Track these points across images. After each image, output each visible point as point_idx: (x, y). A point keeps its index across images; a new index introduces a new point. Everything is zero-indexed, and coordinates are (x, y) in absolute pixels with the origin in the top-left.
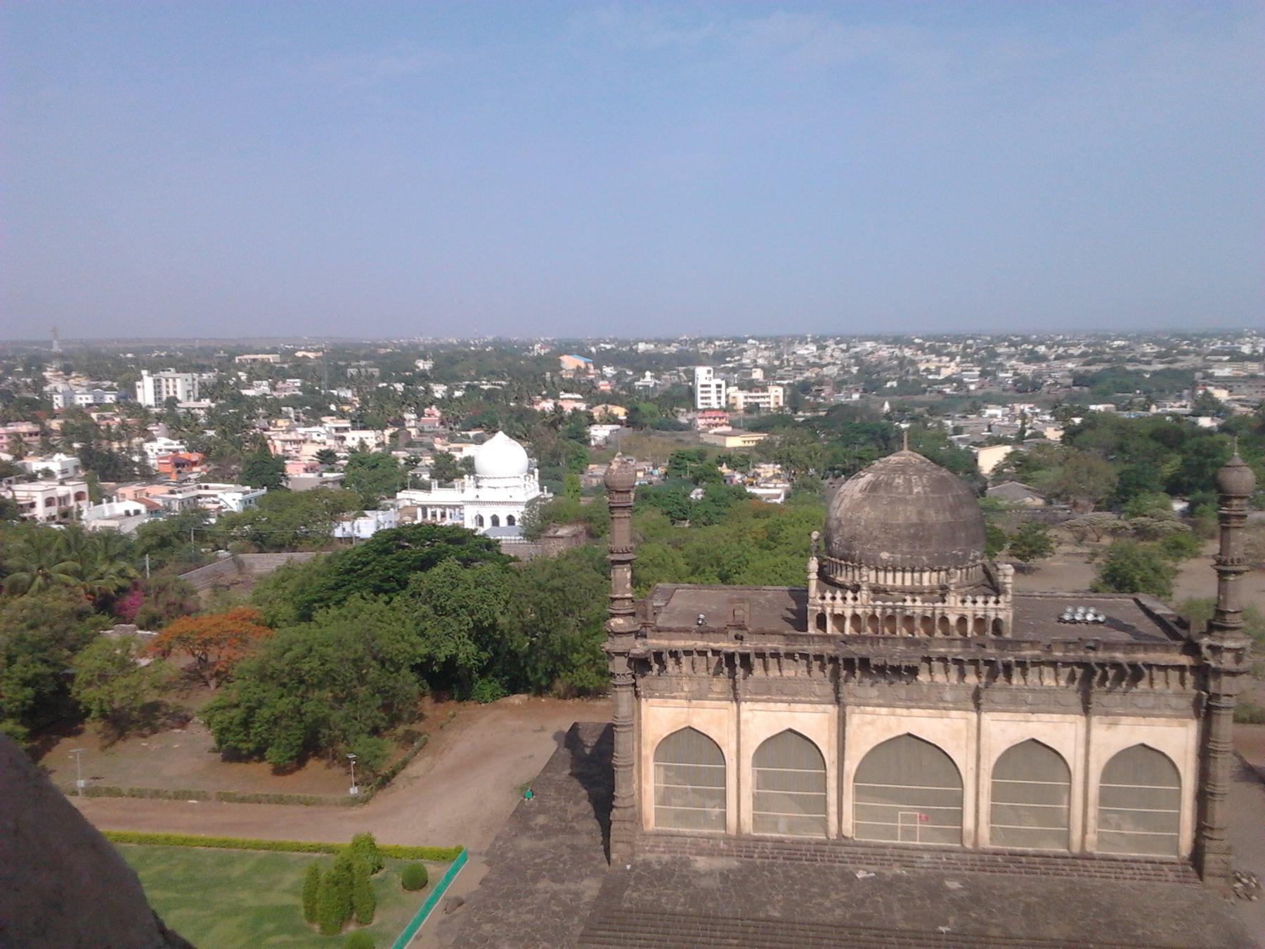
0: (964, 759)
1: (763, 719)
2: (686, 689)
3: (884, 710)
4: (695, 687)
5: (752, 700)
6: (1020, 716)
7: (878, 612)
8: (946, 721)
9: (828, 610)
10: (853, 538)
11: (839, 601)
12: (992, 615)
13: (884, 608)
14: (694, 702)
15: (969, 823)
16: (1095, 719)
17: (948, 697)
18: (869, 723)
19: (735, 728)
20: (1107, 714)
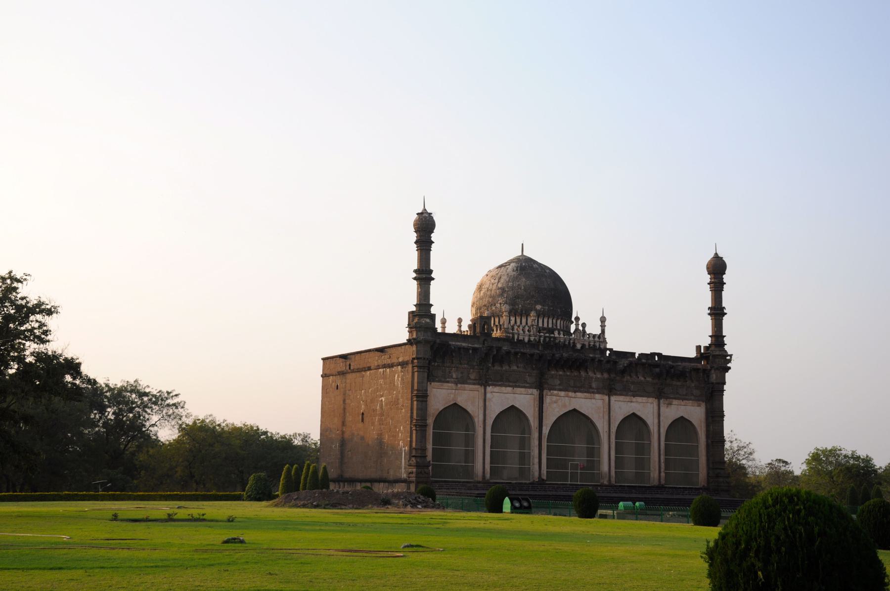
0: (601, 425)
1: (500, 398)
2: (454, 376)
3: (562, 393)
4: (460, 375)
5: (492, 385)
6: (628, 398)
7: (542, 339)
8: (593, 401)
9: (516, 337)
10: (517, 297)
11: (521, 332)
12: (597, 344)
13: (545, 337)
14: (459, 385)
15: (605, 468)
16: (661, 401)
17: (594, 385)
18: (556, 402)
19: (481, 404)
20: (667, 398)
